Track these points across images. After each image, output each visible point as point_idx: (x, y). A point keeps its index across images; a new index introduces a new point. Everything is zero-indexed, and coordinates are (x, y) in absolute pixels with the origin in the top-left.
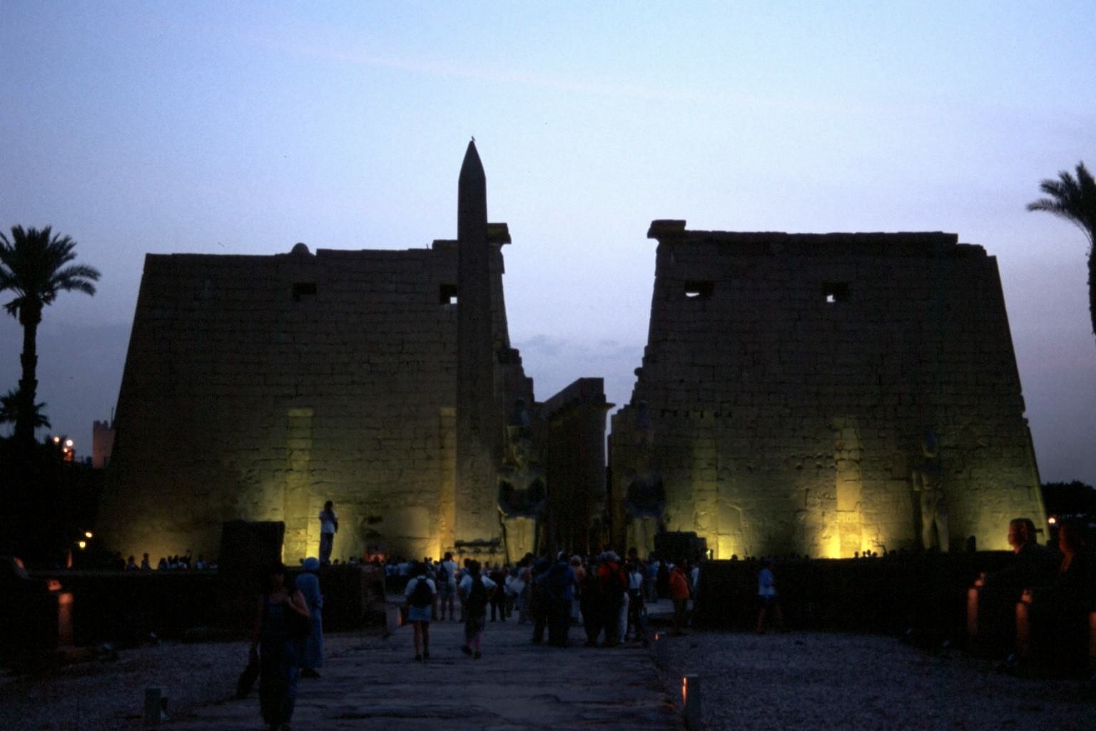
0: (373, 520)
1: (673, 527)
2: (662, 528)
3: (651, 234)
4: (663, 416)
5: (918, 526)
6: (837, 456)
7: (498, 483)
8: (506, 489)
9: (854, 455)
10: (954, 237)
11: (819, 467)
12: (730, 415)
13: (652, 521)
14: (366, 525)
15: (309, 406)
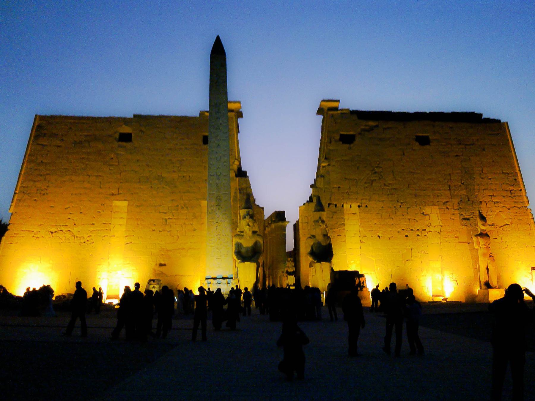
0: (161, 265)
1: (336, 269)
2: (332, 270)
3: (320, 111)
4: (329, 206)
5: (476, 269)
6: (428, 230)
7: (234, 243)
8: (239, 246)
9: (438, 229)
10: (481, 115)
11: (418, 235)
12: (366, 206)
13: (325, 265)
14: (157, 268)
15: (125, 200)
